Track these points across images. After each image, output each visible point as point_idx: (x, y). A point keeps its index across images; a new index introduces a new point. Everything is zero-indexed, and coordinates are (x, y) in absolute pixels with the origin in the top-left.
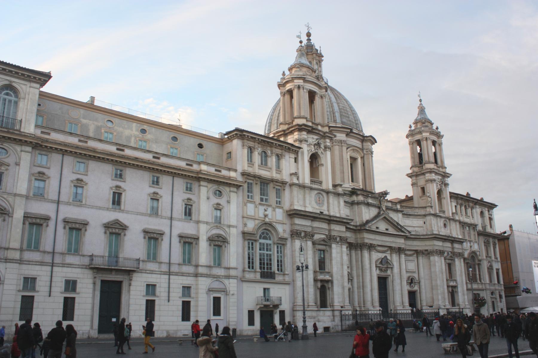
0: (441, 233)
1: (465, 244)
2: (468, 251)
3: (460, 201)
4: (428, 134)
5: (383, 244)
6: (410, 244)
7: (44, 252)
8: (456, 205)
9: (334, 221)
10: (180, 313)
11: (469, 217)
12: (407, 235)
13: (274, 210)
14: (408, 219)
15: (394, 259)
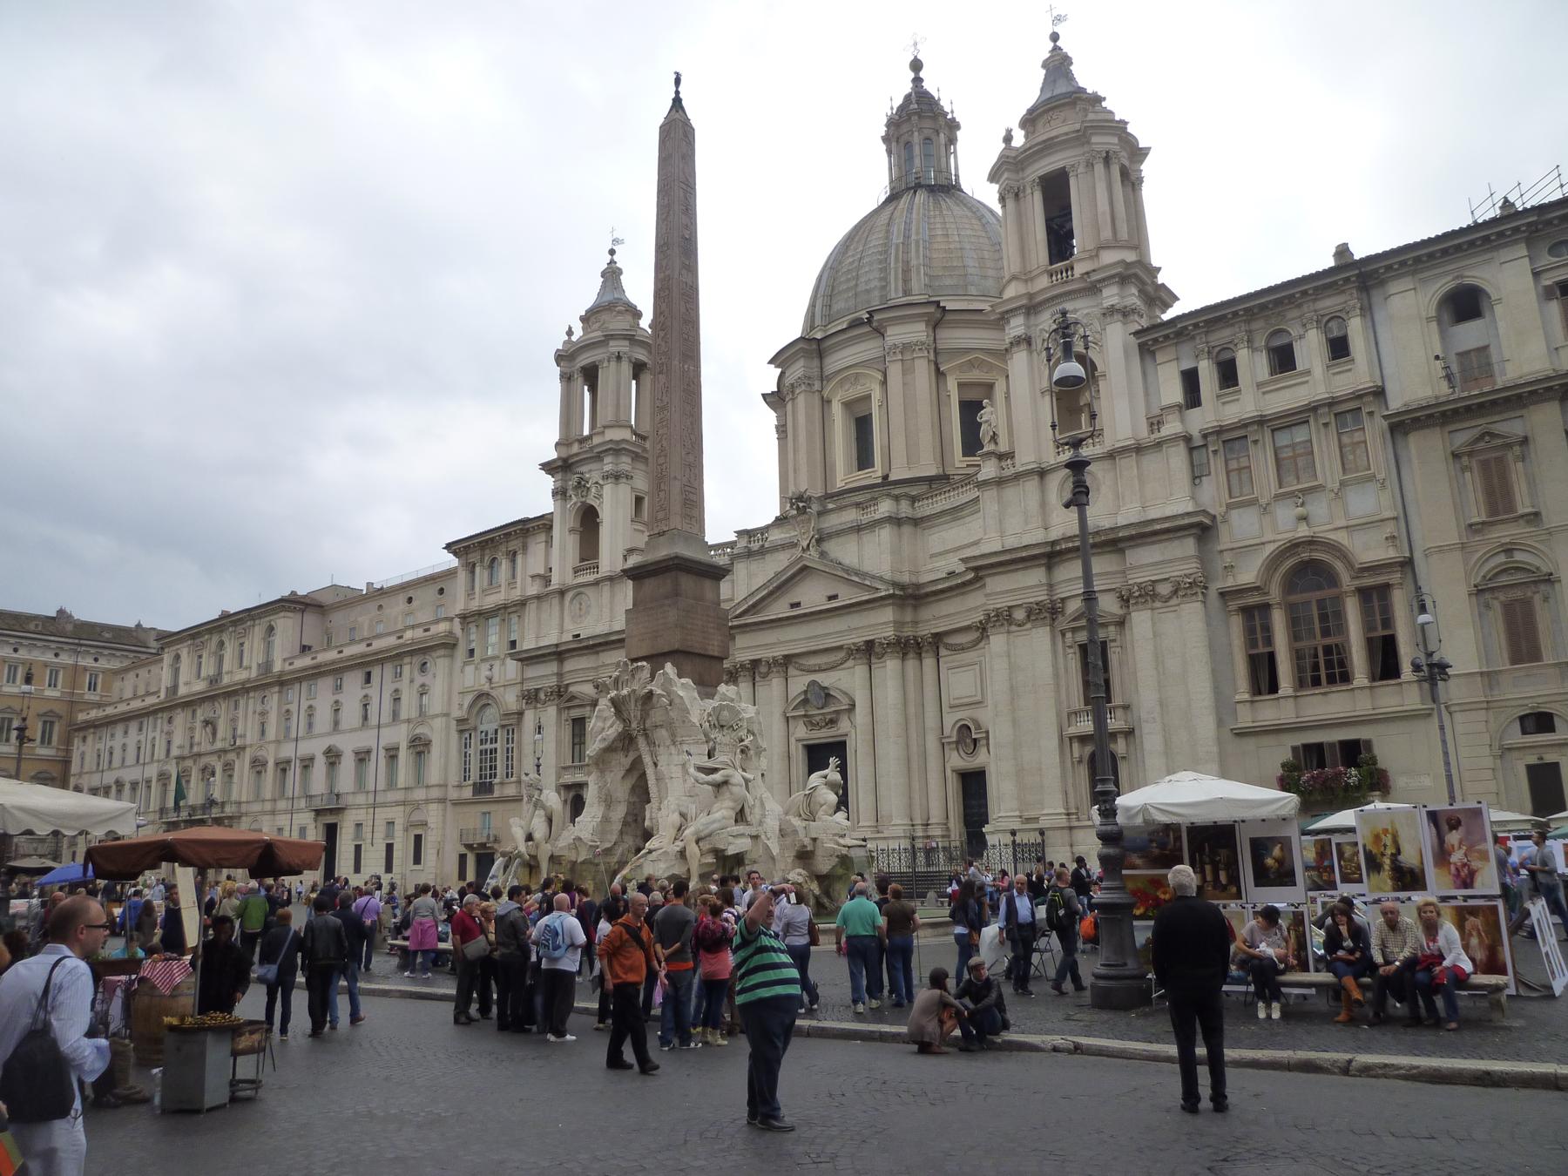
0: (1027, 540)
1: (1242, 527)
2: (1270, 548)
3: (1221, 336)
4: (1006, 175)
5: (813, 646)
6: (952, 611)
7: (288, 799)
8: (1187, 365)
9: (600, 644)
10: (383, 862)
11: (1308, 372)
12: (883, 594)
13: (503, 664)
14: (961, 521)
15: (848, 680)
